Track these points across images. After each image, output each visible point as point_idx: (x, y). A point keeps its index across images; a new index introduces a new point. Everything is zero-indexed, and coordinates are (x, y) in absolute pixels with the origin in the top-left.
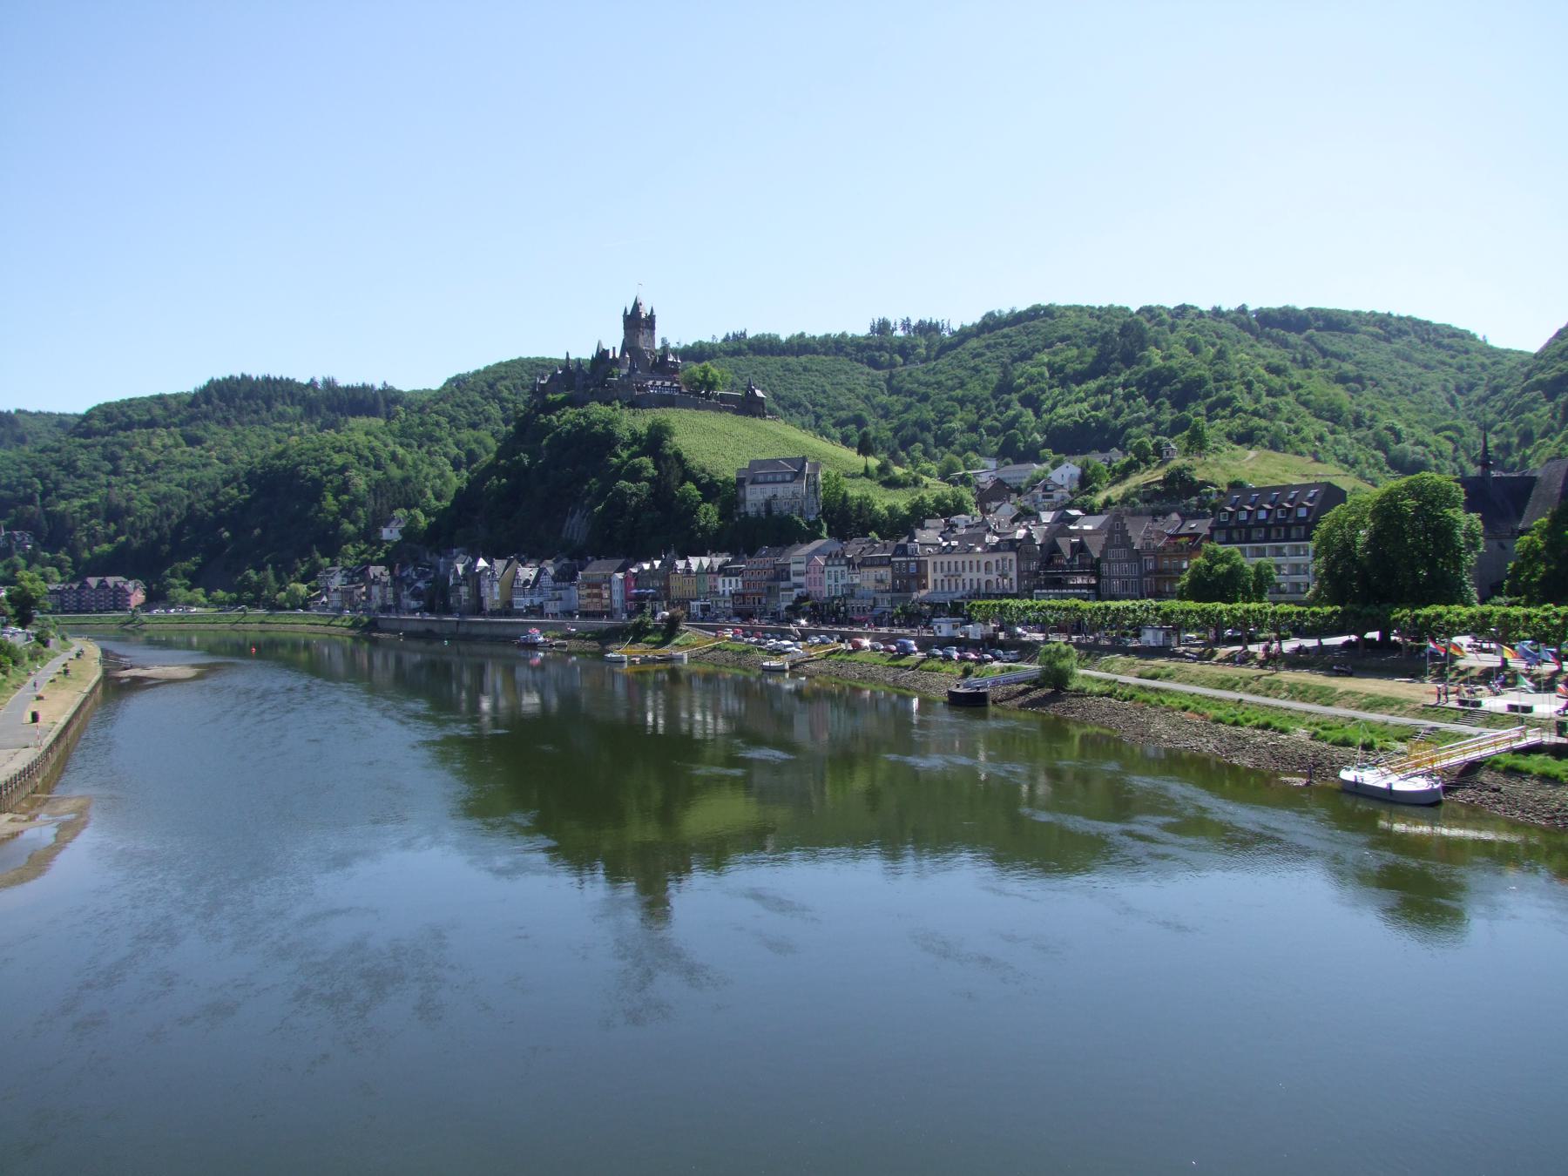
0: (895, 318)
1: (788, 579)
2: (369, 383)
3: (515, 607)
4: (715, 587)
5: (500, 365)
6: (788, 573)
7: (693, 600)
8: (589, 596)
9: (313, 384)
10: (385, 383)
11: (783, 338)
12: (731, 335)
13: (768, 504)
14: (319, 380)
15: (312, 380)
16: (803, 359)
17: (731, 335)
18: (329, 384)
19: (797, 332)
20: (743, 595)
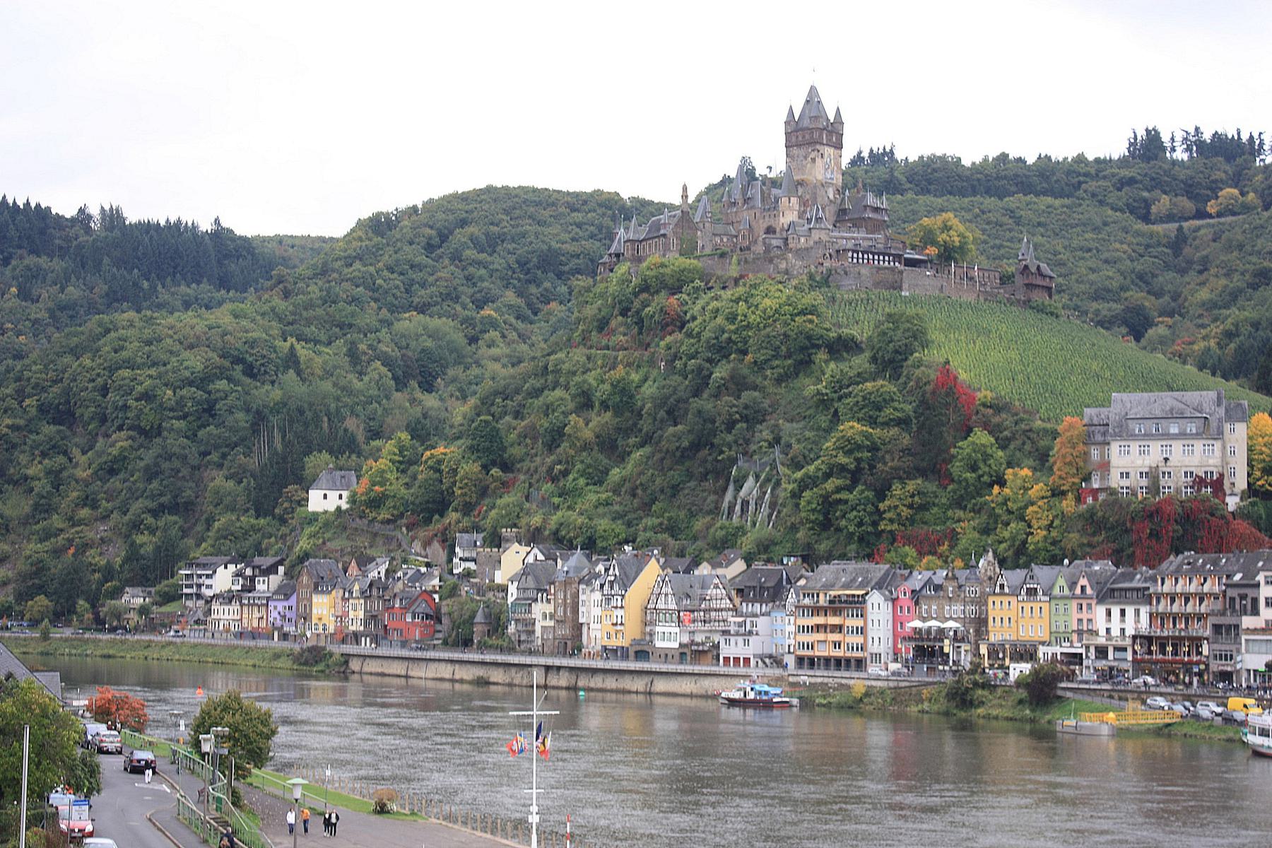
0: (1172, 128)
1: (1255, 612)
2: (187, 218)
3: (659, 644)
4: (1090, 620)
5: (456, 197)
6: (1255, 601)
7: (1043, 643)
8: (818, 628)
9: (83, 217)
10: (217, 221)
11: (970, 158)
12: (866, 154)
13: (1153, 476)
14: (94, 211)
15: (81, 211)
16: (1011, 202)
17: (866, 154)
18: (113, 218)
19: (993, 154)
20: (1149, 640)
